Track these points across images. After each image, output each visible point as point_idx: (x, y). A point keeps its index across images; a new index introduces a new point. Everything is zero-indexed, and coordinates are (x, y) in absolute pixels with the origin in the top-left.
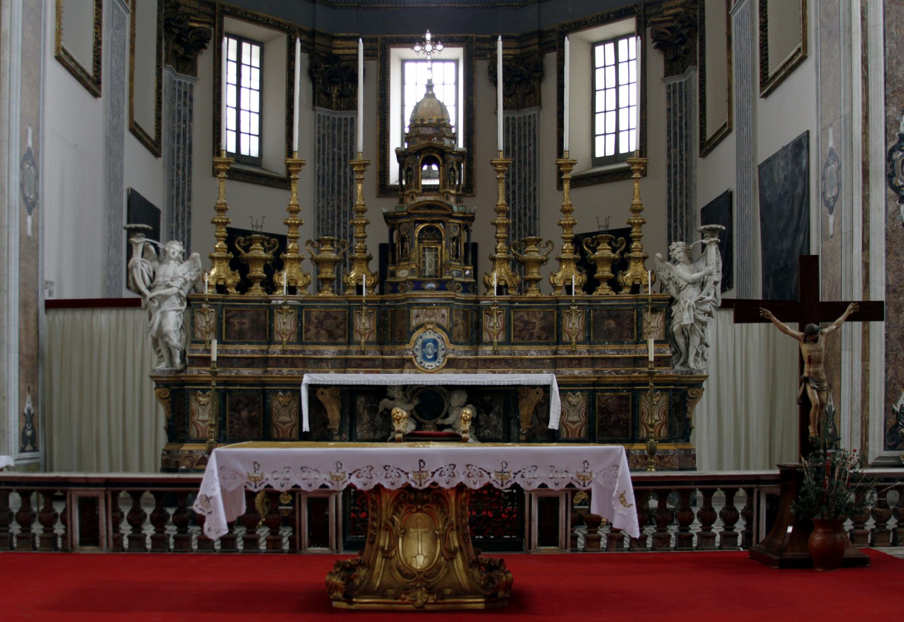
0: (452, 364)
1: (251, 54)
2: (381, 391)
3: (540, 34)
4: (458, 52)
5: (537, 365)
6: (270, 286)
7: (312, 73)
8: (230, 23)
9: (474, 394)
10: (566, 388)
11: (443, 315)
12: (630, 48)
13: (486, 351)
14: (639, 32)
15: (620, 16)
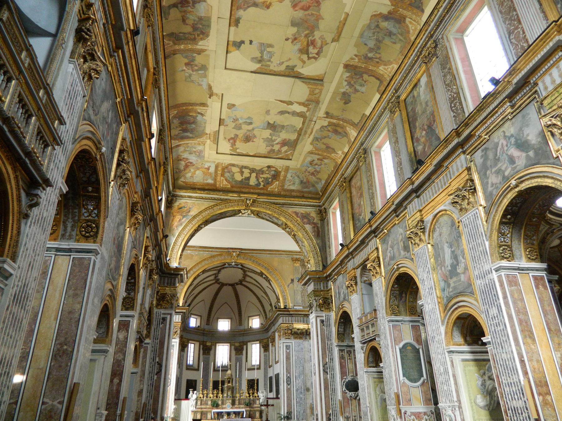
0: (232, 408)
1: (193, 345)
2: (222, 412)
3: (243, 342)
4: (229, 344)
5: (242, 408)
6: (207, 397)
7: (203, 349)
8: (190, 342)
9: (235, 413)
10: (246, 411)
11: (230, 401)
12: (258, 345)
13: (236, 406)
14: (260, 343)
15: (257, 341)
